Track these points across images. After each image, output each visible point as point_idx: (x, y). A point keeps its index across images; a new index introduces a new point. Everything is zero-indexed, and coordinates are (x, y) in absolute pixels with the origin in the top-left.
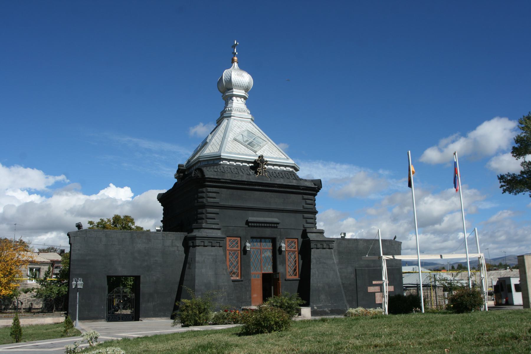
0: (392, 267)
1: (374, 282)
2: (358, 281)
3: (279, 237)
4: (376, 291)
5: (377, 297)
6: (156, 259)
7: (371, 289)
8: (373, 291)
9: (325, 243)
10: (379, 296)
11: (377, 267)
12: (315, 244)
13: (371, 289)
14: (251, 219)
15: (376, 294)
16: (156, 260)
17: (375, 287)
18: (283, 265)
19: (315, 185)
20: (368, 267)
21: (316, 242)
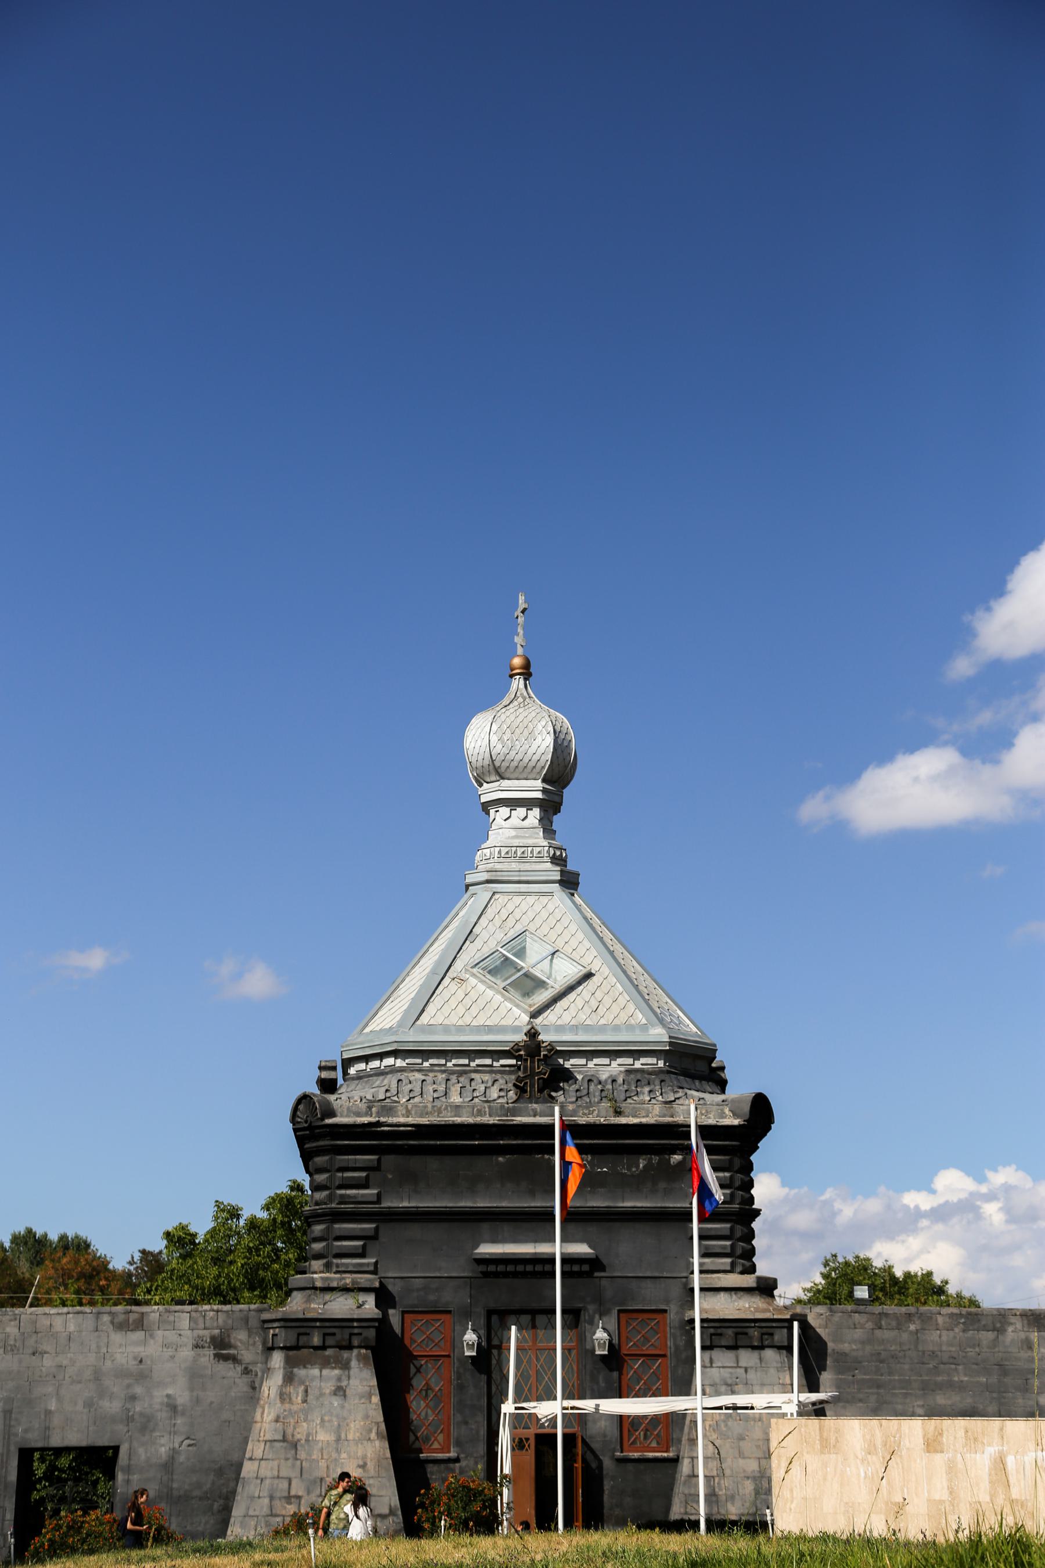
3: (591, 1308)
6: (170, 1391)
14: (487, 1249)
16: (168, 1396)
19: (735, 1115)
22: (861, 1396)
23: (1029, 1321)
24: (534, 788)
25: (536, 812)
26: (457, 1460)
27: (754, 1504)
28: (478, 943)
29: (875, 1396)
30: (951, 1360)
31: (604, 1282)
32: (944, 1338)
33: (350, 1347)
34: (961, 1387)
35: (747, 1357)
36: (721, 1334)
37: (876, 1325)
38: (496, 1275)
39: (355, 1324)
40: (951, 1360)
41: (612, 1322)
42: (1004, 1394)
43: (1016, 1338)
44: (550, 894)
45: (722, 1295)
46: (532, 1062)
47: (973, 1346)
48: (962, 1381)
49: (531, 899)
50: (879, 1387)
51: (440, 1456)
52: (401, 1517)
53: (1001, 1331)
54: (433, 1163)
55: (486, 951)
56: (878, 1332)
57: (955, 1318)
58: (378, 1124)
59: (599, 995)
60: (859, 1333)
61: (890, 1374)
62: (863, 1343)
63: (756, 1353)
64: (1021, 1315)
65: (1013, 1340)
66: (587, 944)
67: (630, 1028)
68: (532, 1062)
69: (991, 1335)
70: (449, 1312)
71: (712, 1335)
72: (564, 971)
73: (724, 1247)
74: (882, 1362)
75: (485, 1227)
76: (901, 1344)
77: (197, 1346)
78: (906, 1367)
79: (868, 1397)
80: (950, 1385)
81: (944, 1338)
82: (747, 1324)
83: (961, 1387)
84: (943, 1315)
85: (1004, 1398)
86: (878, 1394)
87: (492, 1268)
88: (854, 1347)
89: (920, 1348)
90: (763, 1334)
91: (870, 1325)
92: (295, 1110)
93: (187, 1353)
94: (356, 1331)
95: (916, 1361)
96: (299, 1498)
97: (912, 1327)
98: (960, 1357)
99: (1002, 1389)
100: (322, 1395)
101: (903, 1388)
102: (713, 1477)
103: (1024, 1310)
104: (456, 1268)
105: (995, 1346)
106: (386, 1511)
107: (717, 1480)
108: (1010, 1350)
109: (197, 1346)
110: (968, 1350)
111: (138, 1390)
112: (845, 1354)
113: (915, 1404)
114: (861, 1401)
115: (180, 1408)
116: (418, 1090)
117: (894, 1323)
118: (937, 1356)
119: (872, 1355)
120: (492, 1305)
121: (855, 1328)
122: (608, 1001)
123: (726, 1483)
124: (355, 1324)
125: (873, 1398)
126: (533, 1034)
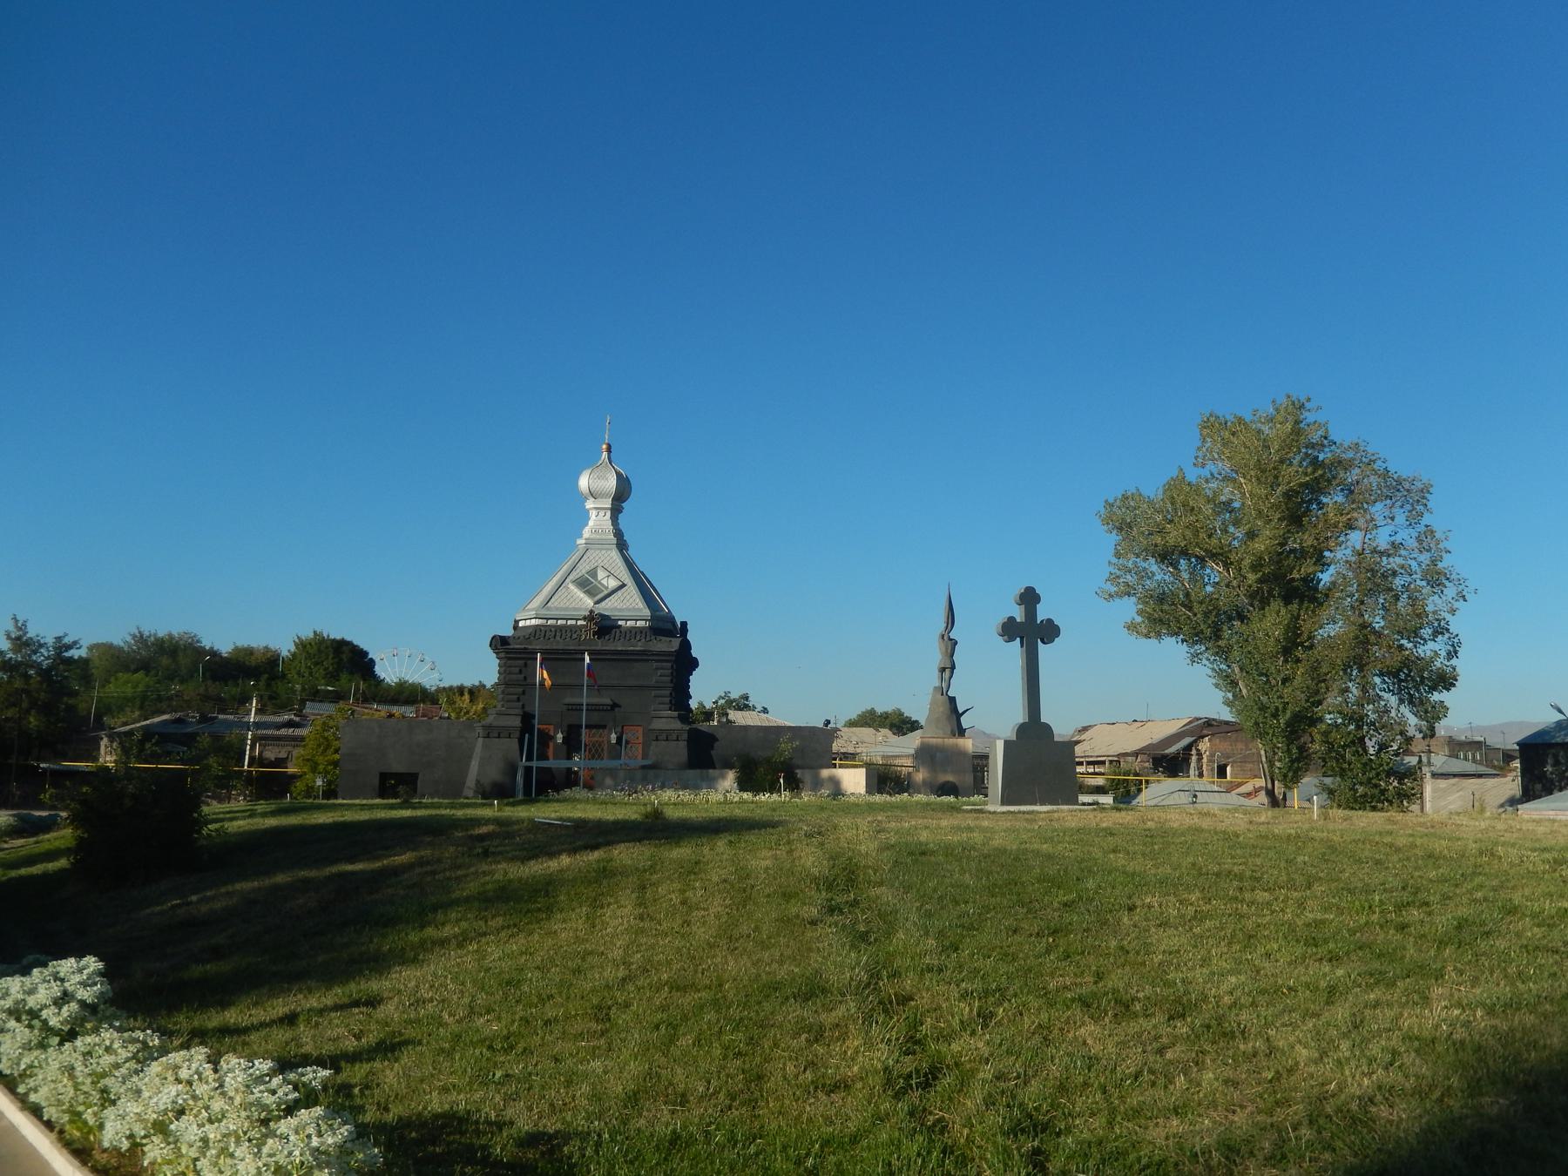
24: (608, 503)
25: (609, 513)
28: (578, 571)
44: (611, 549)
45: (664, 720)
49: (603, 552)
55: (580, 574)
58: (525, 649)
59: (625, 595)
66: (624, 572)
67: (634, 609)
72: (613, 583)
92: (491, 642)
116: (543, 635)
122: (628, 597)
126: (591, 611)
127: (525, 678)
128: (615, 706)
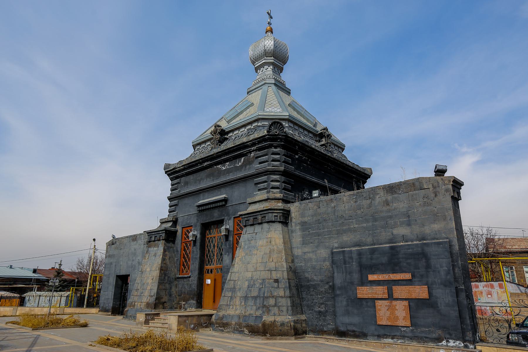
0: (424, 239)
1: (371, 277)
2: (336, 274)
3: (226, 218)
4: (376, 296)
5: (380, 310)
7: (364, 292)
8: (370, 296)
9: (261, 214)
10: (387, 308)
11: (381, 244)
12: (246, 219)
13: (364, 292)
14: (201, 202)
15: (378, 303)
17: (375, 287)
18: (228, 255)
20: (359, 245)
21: (247, 216)
22: (311, 241)
23: (387, 190)
26: (190, 277)
27: (246, 292)
29: (318, 240)
30: (350, 218)
31: (230, 208)
32: (347, 207)
33: (159, 240)
34: (355, 230)
35: (258, 228)
36: (249, 220)
37: (318, 206)
38: (204, 210)
39: (160, 232)
40: (350, 218)
41: (231, 222)
42: (375, 231)
43: (381, 201)
46: (215, 136)
47: (360, 209)
48: (355, 227)
50: (319, 236)
51: (186, 276)
52: (155, 296)
53: (373, 199)
54: (191, 177)
56: (319, 210)
57: (351, 196)
60: (311, 212)
61: (324, 228)
62: (312, 216)
63: (260, 226)
64: (383, 188)
65: (379, 202)
68: (215, 136)
69: (368, 202)
70: (192, 226)
71: (246, 221)
73: (264, 186)
74: (320, 224)
75: (202, 195)
76: (328, 214)
77: (144, 245)
78: (330, 224)
79: (314, 241)
80: (350, 230)
81: (347, 207)
82: (256, 214)
83: (355, 230)
84: (346, 196)
85: (375, 233)
86: (318, 239)
87: (203, 208)
88: (309, 218)
89: (336, 214)
90: (262, 217)
91: (316, 207)
93: (142, 246)
94: (161, 234)
95: (334, 221)
96: (138, 289)
97: (333, 205)
98: (354, 215)
99: (374, 229)
100: (151, 256)
101: (329, 235)
102: (236, 280)
103: (385, 185)
104: (194, 211)
105: (370, 207)
106: (153, 295)
107: (237, 281)
108: (377, 207)
109: (144, 245)
110: (358, 211)
111: (134, 258)
112: (306, 222)
113: (334, 242)
114: (311, 243)
115: (140, 263)
117: (325, 204)
118: (343, 217)
119: (316, 221)
120: (202, 222)
121: (310, 210)
123: (239, 283)
124: (160, 232)
125: (316, 241)
127: (180, 191)
128: (225, 200)
